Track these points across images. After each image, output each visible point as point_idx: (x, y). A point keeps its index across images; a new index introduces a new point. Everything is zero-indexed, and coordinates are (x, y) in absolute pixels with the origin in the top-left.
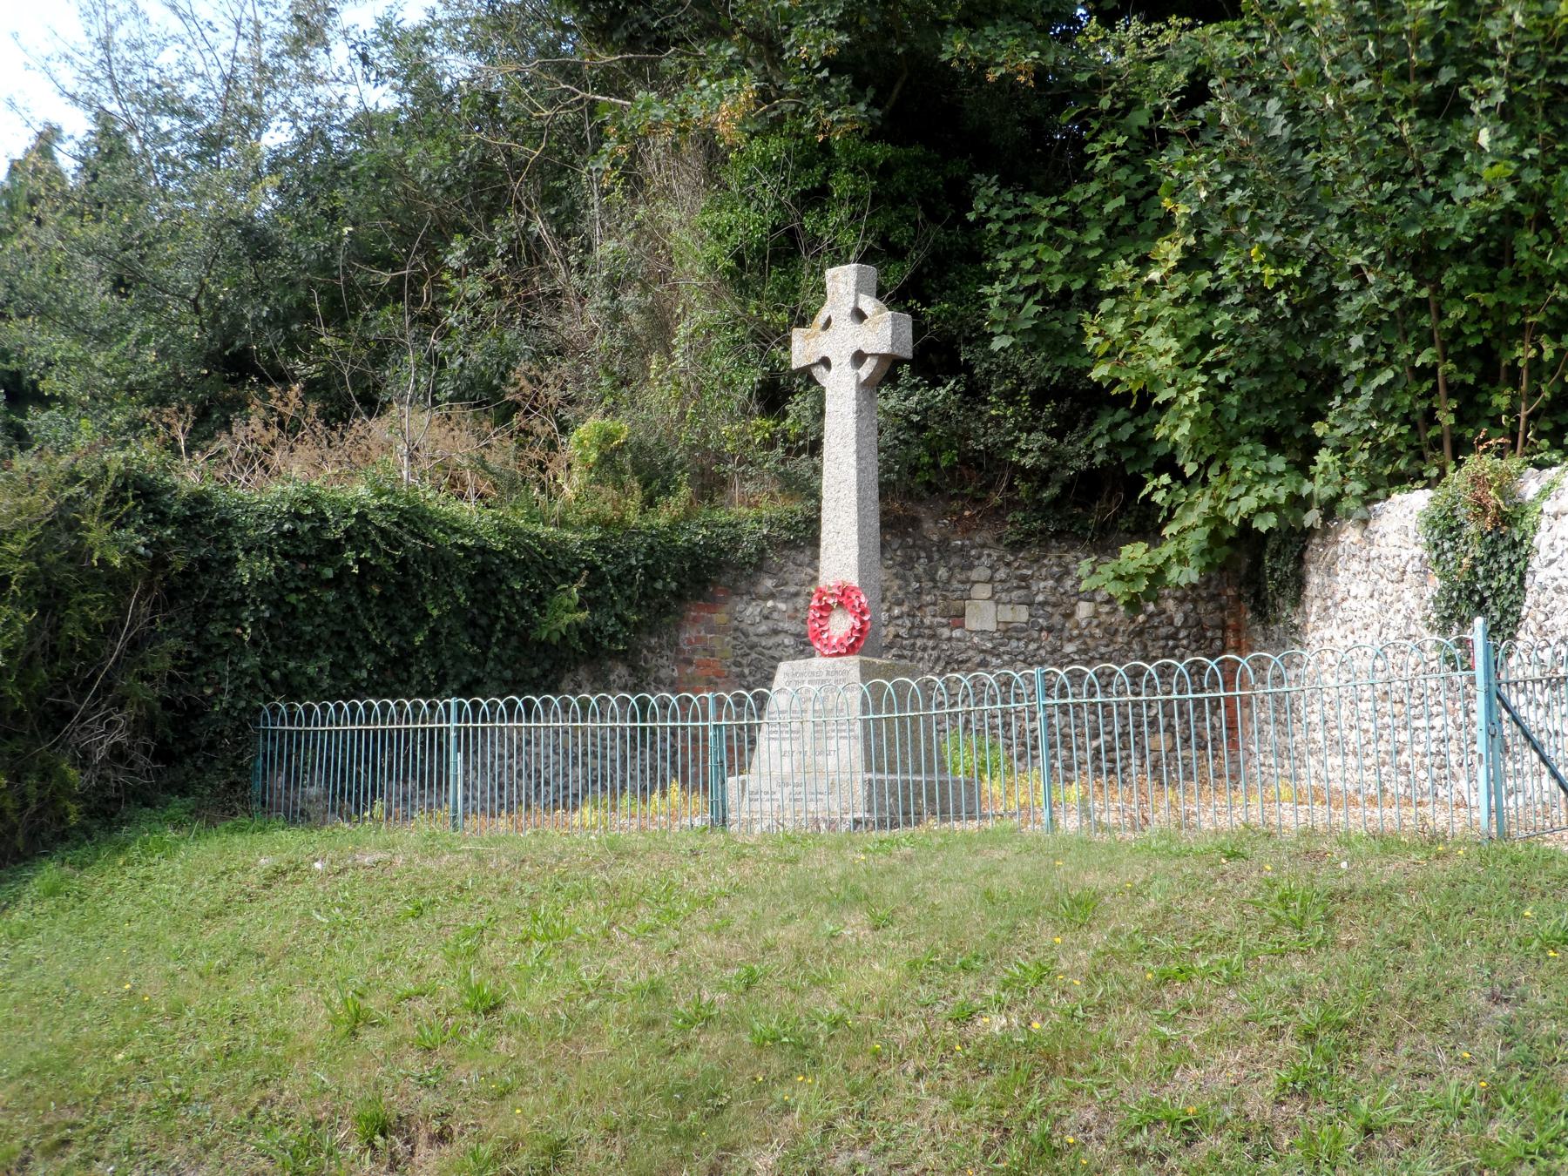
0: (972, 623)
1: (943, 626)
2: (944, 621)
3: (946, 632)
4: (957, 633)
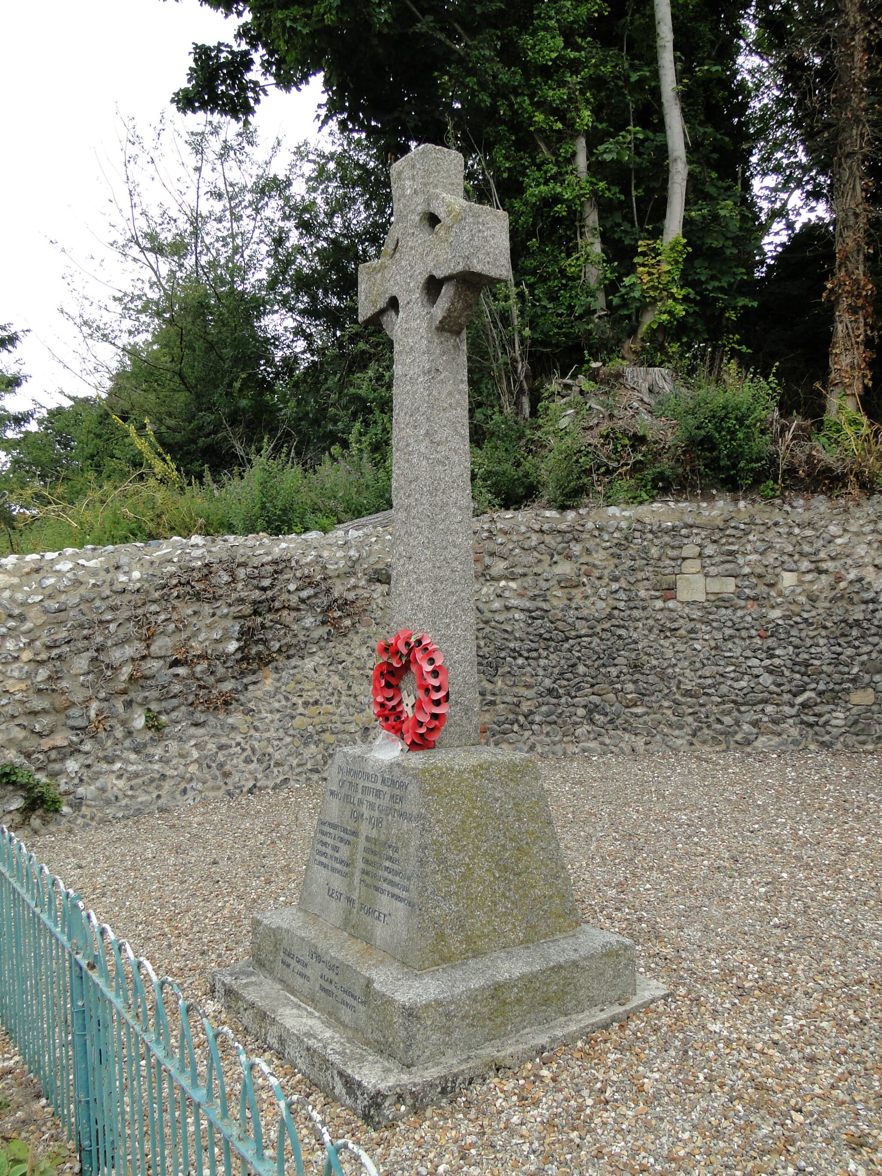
0: (683, 594)
1: (657, 598)
2: (657, 594)
3: (659, 604)
4: (671, 604)
